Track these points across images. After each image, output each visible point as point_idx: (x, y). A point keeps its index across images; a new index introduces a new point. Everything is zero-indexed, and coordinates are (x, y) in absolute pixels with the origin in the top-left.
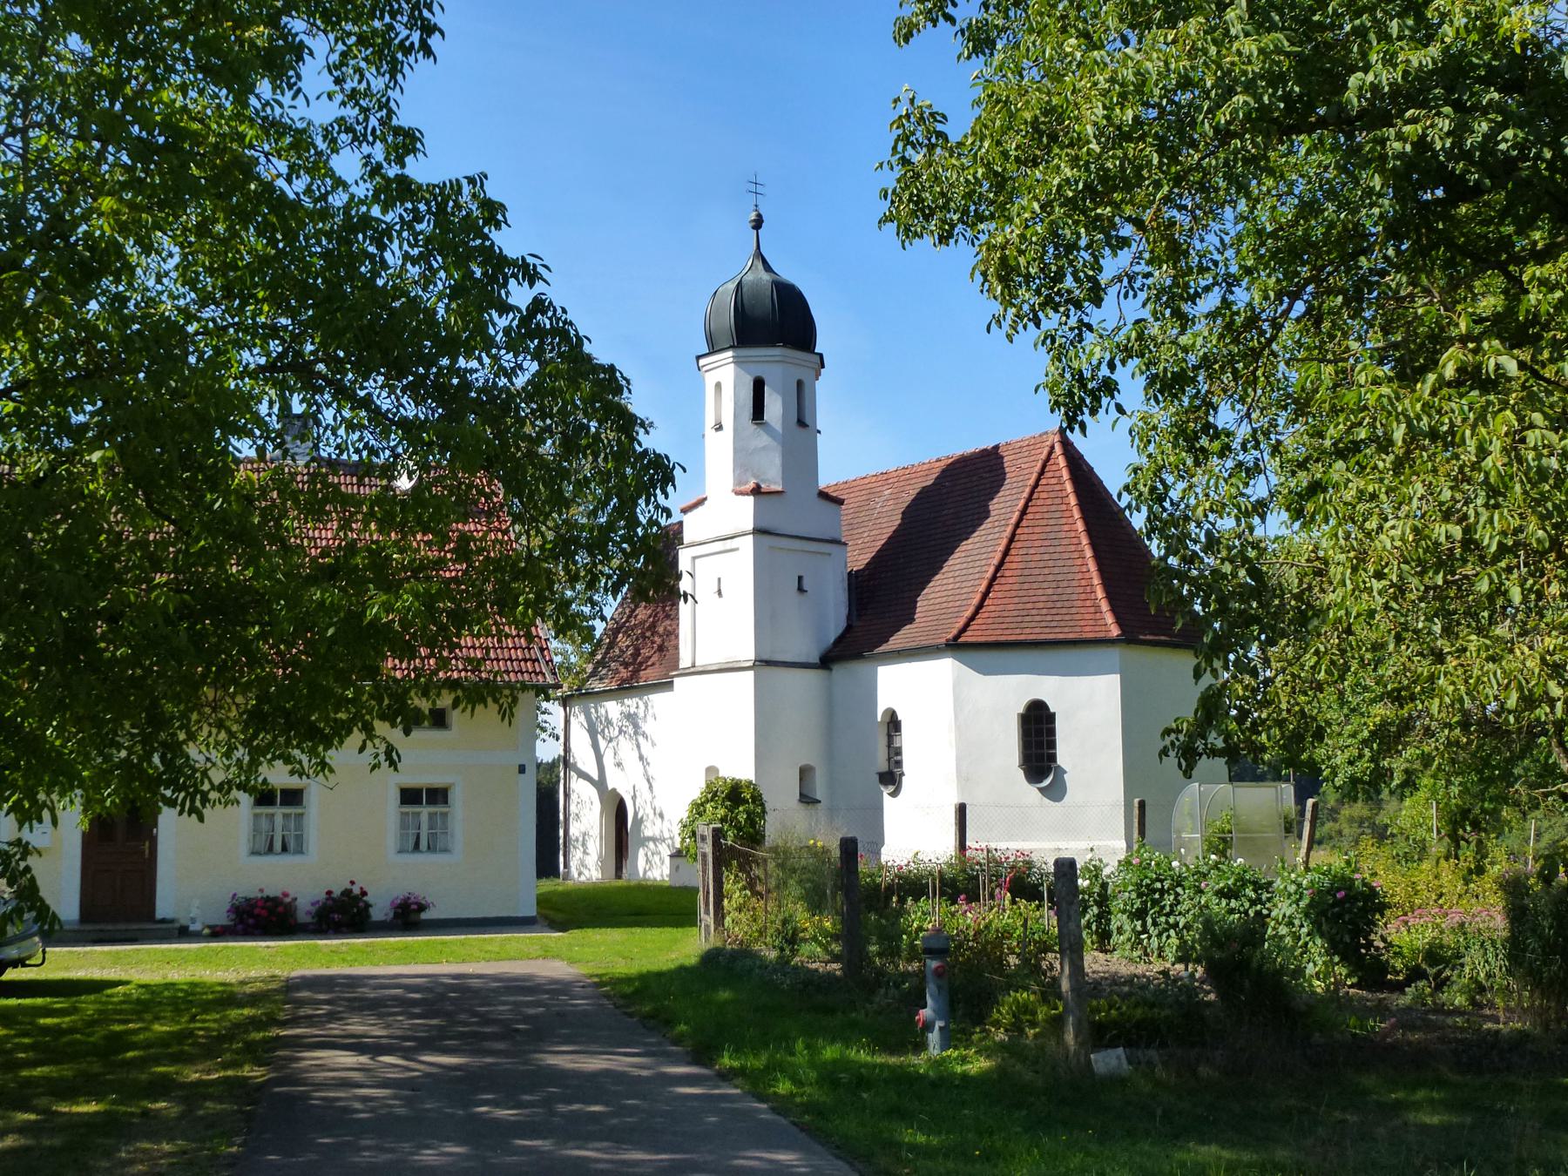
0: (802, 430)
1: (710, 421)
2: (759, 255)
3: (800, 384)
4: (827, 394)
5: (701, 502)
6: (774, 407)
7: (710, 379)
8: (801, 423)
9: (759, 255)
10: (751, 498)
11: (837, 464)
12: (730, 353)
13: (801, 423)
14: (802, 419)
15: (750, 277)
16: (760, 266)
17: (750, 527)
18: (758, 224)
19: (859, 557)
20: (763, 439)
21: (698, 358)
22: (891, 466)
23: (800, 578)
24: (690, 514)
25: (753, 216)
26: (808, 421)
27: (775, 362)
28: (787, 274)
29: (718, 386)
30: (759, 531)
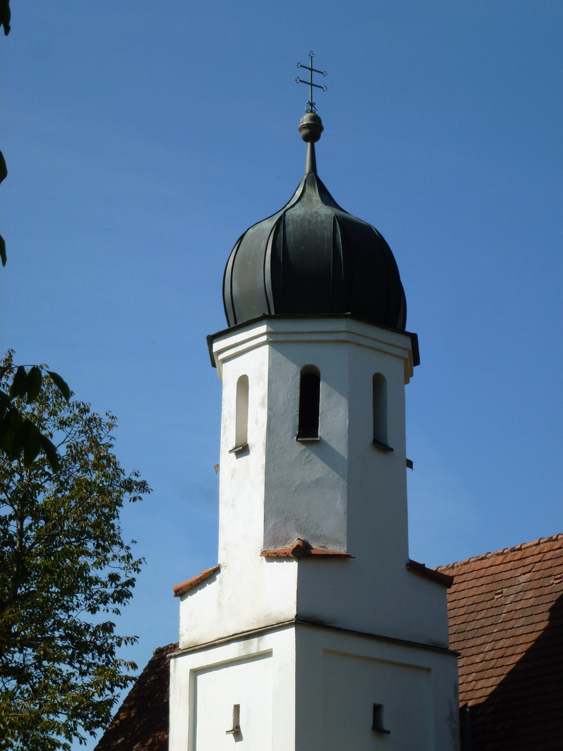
0: (379, 458)
1: (228, 439)
2: (314, 178)
3: (378, 381)
4: (421, 402)
5: (210, 576)
6: (335, 416)
7: (230, 373)
8: (381, 445)
9: (314, 178)
10: (292, 567)
11: (442, 527)
12: (263, 328)
13: (381, 445)
14: (381, 438)
15: (298, 211)
16: (315, 196)
17: (290, 610)
18: (313, 131)
19: (477, 684)
20: (316, 468)
21: (211, 339)
22: (528, 536)
23: (377, 709)
24: (191, 600)
25: (306, 119)
26: (391, 443)
27: (342, 349)
28: (359, 210)
29: (243, 383)
30: (303, 622)
